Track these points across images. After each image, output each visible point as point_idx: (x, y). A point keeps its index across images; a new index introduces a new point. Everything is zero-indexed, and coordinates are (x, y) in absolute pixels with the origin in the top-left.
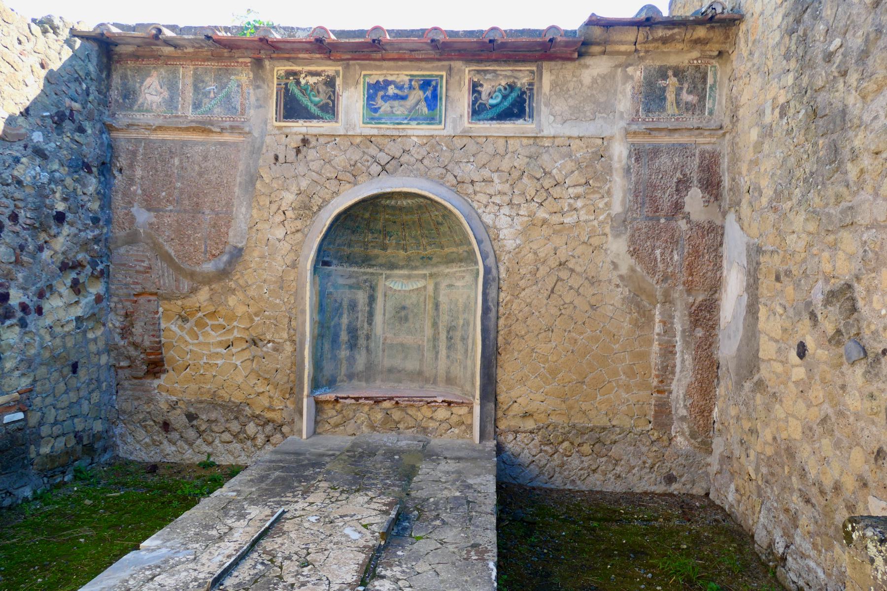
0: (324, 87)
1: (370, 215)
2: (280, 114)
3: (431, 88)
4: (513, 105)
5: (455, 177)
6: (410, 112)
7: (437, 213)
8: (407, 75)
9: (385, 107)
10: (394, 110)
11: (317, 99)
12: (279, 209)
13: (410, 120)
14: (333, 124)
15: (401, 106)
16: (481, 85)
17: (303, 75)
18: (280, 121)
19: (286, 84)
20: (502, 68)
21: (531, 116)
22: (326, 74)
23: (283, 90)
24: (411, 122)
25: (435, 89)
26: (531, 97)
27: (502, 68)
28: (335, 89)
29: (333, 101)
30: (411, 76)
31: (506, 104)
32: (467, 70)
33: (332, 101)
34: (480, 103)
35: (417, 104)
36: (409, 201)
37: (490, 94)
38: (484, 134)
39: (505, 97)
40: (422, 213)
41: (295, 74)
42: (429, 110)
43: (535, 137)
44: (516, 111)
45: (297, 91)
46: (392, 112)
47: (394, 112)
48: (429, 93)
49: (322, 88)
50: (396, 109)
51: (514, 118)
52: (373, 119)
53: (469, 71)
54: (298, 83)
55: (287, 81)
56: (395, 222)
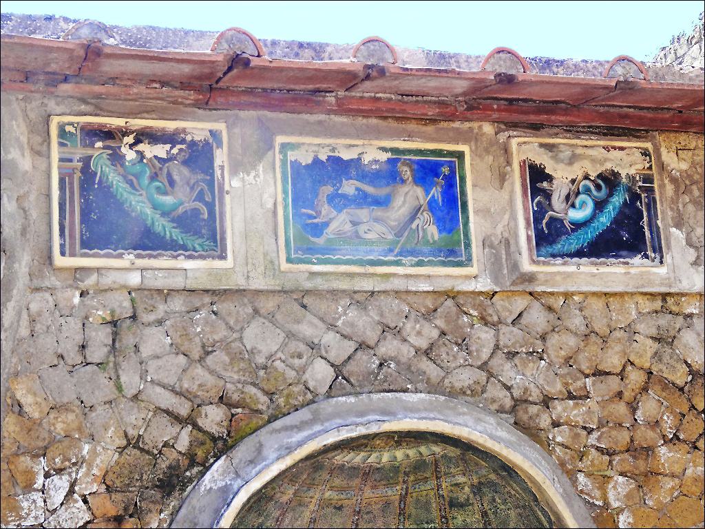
0: (186, 171)
1: (294, 494)
2: (72, 236)
3: (440, 180)
4: (617, 221)
5: (508, 388)
6: (399, 234)
7: (461, 479)
8: (384, 149)
9: (339, 222)
10: (362, 229)
11: (168, 200)
12: (71, 491)
13: (400, 254)
14: (218, 264)
15: (377, 220)
16: (549, 178)
17: (130, 139)
18: (73, 255)
19: (87, 161)
20: (585, 143)
21: (658, 249)
22: (189, 138)
23: (78, 175)
24: (404, 260)
25: (450, 183)
26: (651, 205)
27: (585, 143)
28: (212, 175)
29: (211, 207)
30: (394, 151)
31: (605, 220)
32: (514, 142)
33: (206, 204)
34: (552, 219)
35: (413, 217)
36: (399, 454)
37: (568, 197)
38: (562, 290)
39: (600, 206)
40: (417, 481)
41: (108, 134)
42: (440, 231)
43: (664, 296)
44: (625, 236)
45: (113, 177)
46: (358, 236)
47: (361, 233)
48: (436, 192)
49: (180, 173)
50: (362, 229)
51: (624, 253)
52: (311, 250)
53: (519, 144)
54: (117, 158)
55: (89, 152)
56: (340, 508)
